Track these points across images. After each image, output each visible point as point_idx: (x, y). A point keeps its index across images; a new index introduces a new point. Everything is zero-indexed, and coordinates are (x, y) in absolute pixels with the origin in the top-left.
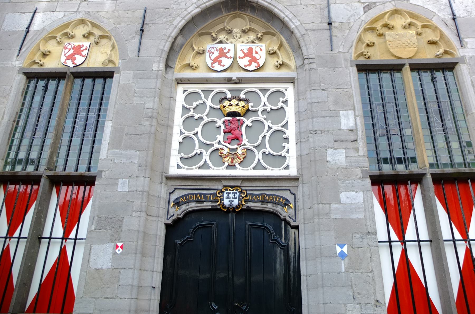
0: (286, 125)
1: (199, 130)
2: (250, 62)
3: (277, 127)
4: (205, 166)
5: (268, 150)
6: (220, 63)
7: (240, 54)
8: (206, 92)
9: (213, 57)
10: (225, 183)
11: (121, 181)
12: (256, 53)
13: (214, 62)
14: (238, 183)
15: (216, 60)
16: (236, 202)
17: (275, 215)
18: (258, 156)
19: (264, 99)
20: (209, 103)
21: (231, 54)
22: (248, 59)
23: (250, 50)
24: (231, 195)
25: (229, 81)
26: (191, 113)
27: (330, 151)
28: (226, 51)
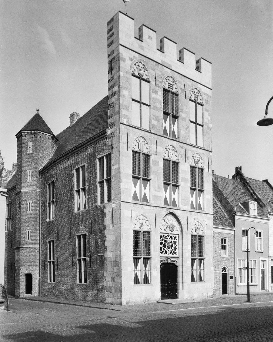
0: (176, 245)
1: (163, 245)
3: (175, 245)
4: (164, 254)
5: (174, 251)
6: (167, 229)
7: (171, 227)
8: (164, 236)
10: (168, 258)
11: (156, 259)
14: (170, 258)
15: (166, 228)
16: (169, 262)
17: (174, 264)
18: (172, 252)
19: (173, 238)
20: (164, 239)
25: (168, 234)
26: (161, 241)
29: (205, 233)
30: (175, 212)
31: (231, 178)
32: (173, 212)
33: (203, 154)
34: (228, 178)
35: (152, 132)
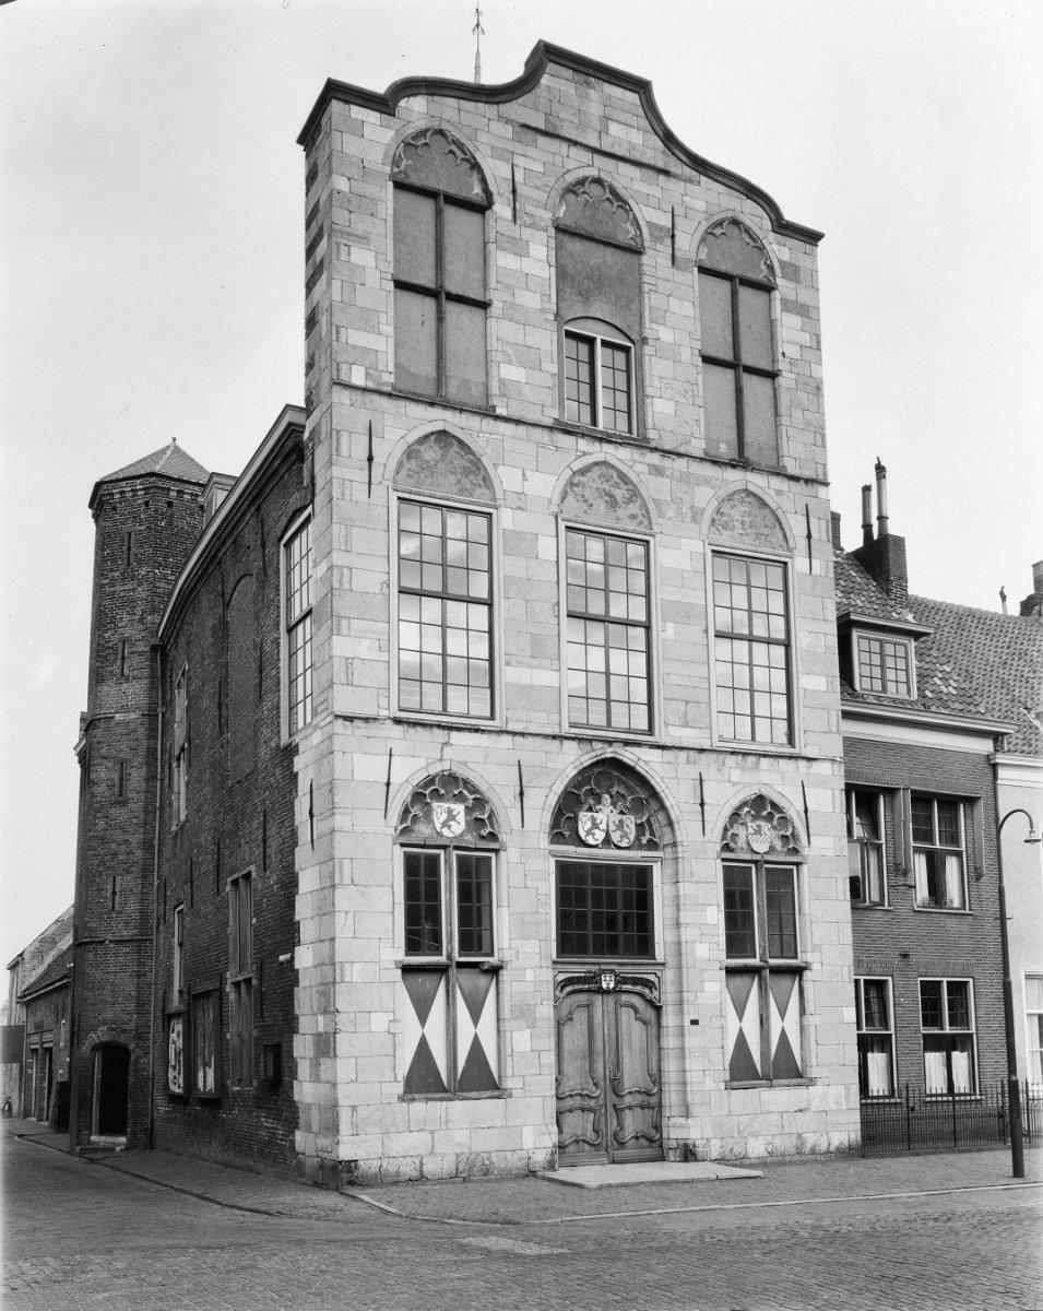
2: (622, 837)
6: (593, 835)
7: (612, 827)
9: (586, 828)
12: (627, 826)
13: (588, 835)
15: (589, 832)
16: (612, 985)
21: (603, 826)
22: (619, 833)
23: (621, 822)
24: (608, 978)
27: (698, 945)
28: (598, 821)
29: (806, 851)
30: (629, 756)
31: (1014, 609)
32: (621, 757)
33: (779, 492)
34: (1000, 612)
35: (499, 411)
